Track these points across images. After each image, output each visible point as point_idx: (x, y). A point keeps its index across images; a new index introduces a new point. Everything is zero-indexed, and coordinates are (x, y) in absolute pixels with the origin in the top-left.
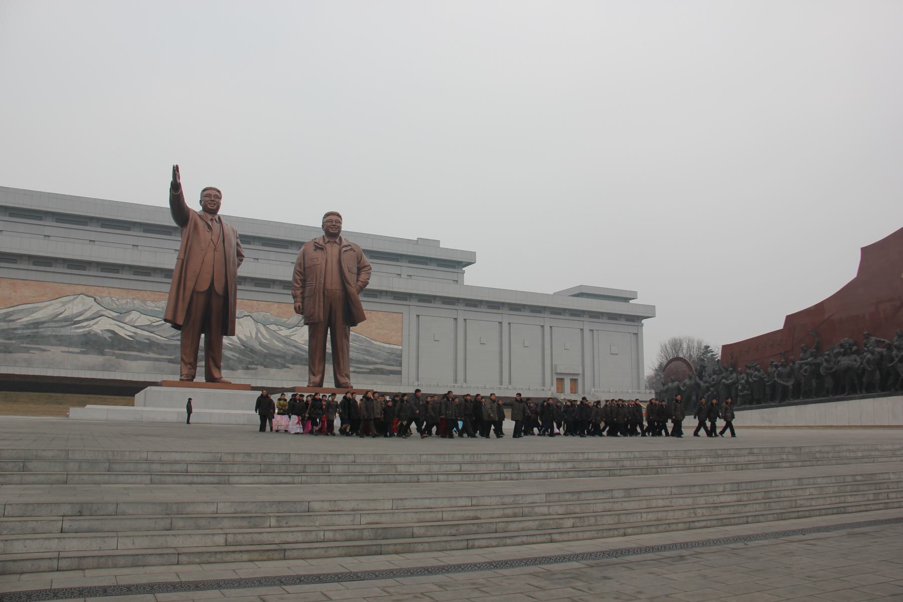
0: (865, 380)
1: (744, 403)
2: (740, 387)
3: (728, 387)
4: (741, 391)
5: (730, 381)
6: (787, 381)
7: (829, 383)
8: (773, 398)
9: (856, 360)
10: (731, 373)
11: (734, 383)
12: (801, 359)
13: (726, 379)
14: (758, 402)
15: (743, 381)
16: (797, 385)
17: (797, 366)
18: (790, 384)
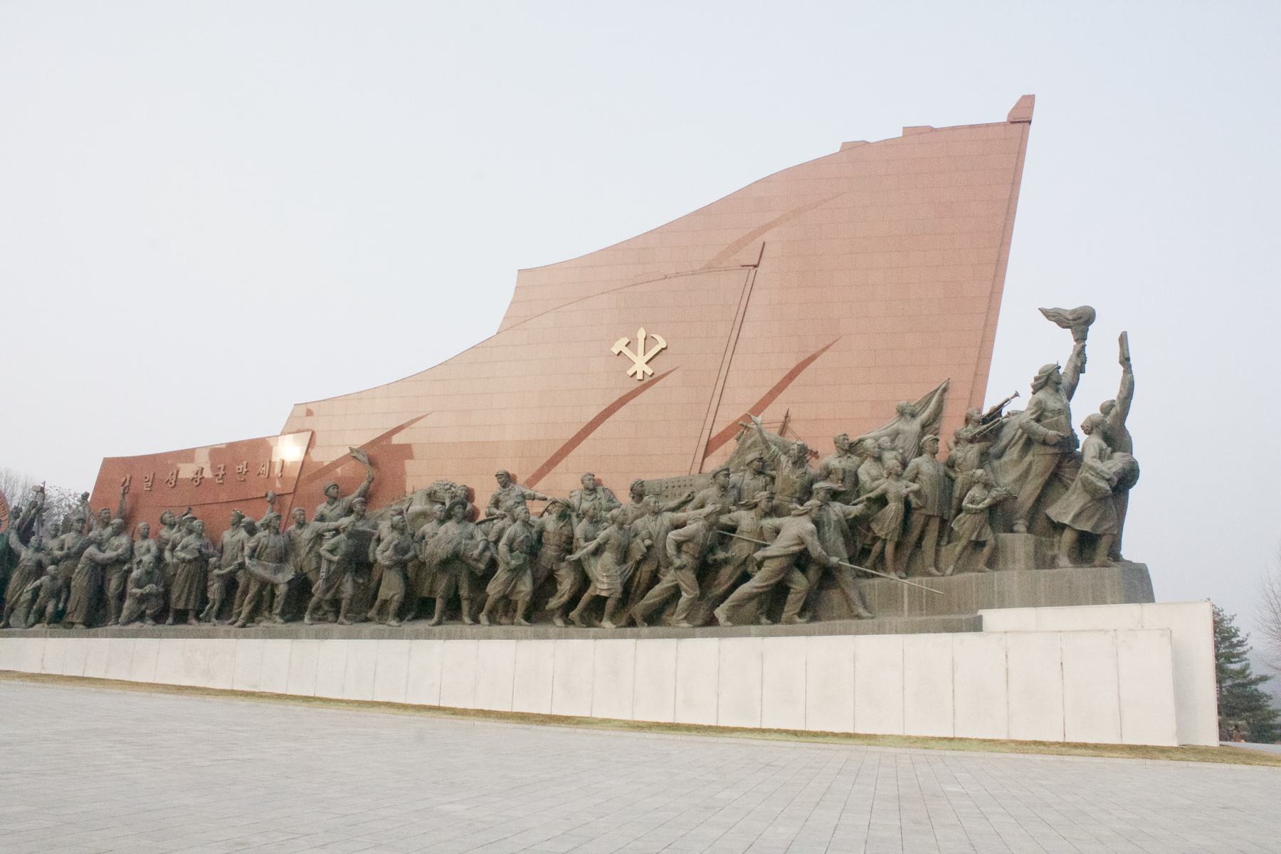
0: (494, 589)
1: (141, 617)
2: (135, 573)
3: (100, 570)
4: (139, 584)
5: (110, 554)
6: (277, 571)
7: (392, 588)
8: (224, 612)
9: (472, 537)
10: (117, 533)
11: (119, 561)
12: (322, 518)
13: (100, 545)
14: (181, 617)
15: (147, 558)
16: (301, 587)
17: (306, 534)
18: (284, 577)
